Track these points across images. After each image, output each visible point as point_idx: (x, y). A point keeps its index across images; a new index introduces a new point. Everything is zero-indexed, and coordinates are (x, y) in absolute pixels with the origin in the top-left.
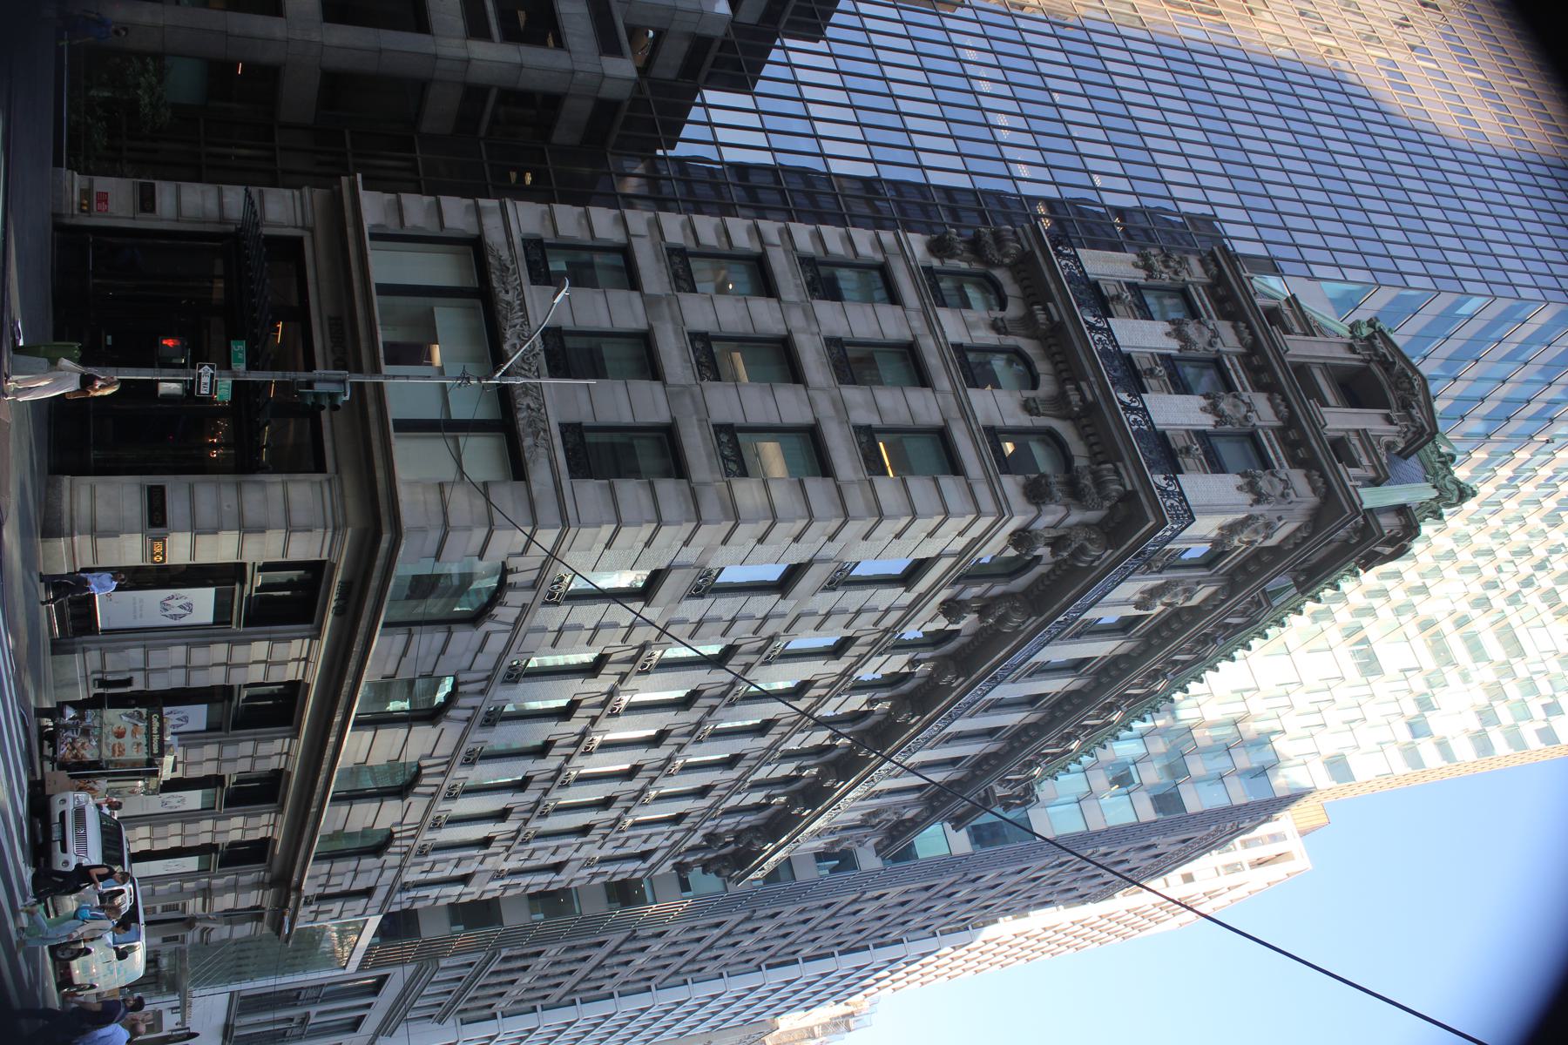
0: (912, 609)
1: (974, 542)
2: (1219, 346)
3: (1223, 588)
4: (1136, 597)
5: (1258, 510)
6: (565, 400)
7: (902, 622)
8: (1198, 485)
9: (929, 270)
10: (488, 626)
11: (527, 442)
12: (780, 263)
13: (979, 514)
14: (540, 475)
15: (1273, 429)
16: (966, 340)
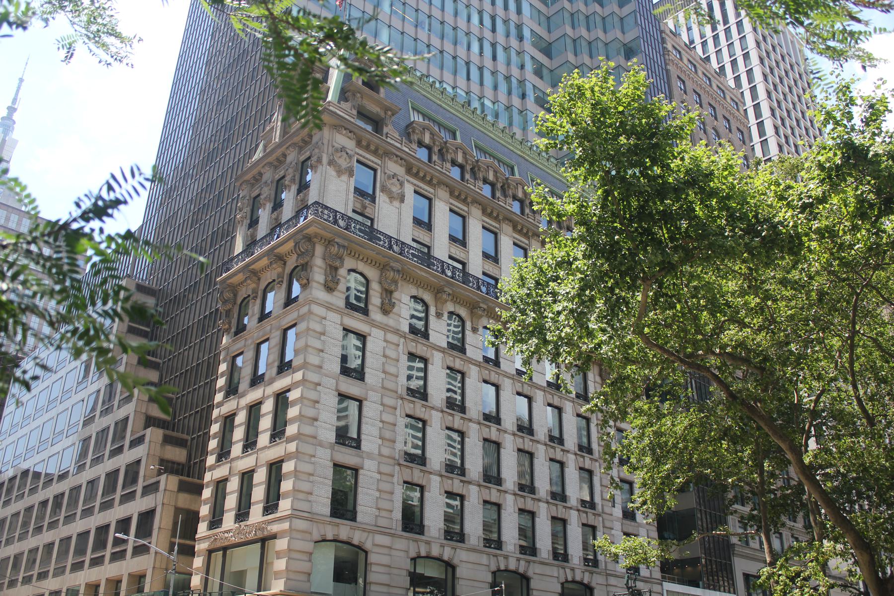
0: (385, 328)
1: (328, 308)
2: (269, 182)
3: (390, 159)
4: (396, 203)
5: (325, 160)
6: (256, 514)
7: (397, 332)
8: (313, 196)
9: (236, 334)
10: (368, 546)
11: (266, 533)
12: (226, 409)
13: (310, 312)
14: (275, 528)
15: (299, 153)
16: (257, 316)
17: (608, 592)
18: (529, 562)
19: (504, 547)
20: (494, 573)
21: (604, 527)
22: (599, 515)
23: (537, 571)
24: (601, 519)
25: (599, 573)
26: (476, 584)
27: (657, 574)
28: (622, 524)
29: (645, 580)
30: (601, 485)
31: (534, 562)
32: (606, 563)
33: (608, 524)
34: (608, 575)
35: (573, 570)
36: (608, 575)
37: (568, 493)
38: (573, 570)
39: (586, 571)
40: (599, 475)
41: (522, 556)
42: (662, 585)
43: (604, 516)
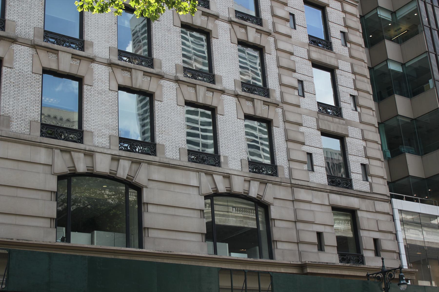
17: (295, 210)
18: (138, 162)
19: (86, 138)
20: (61, 178)
21: (286, 121)
22: (277, 105)
23: (155, 177)
24: (279, 110)
25: (279, 184)
26: (20, 193)
27: (382, 188)
28: (317, 120)
29: (361, 196)
30: (279, 67)
31: (149, 163)
32: (290, 170)
33: (291, 117)
34: (293, 186)
35: (227, 177)
36: (293, 186)
37: (217, 71)
38: (227, 177)
39: (254, 179)
40: (274, 52)
41: (124, 153)
42: (391, 202)
43: (286, 107)
